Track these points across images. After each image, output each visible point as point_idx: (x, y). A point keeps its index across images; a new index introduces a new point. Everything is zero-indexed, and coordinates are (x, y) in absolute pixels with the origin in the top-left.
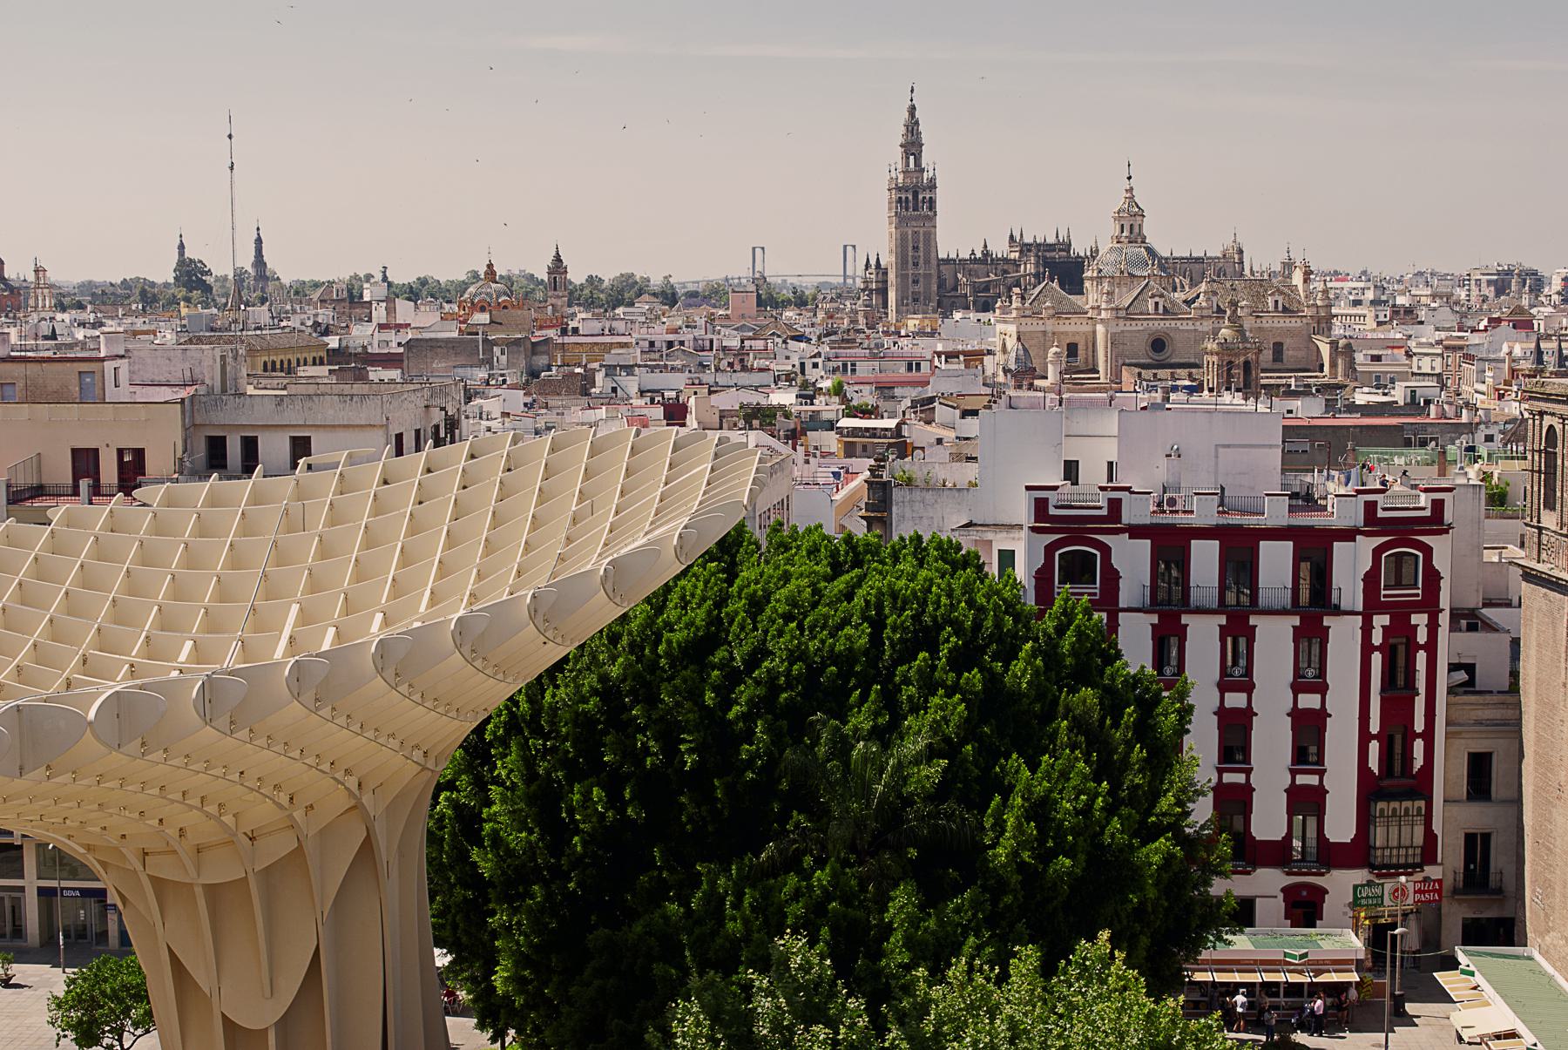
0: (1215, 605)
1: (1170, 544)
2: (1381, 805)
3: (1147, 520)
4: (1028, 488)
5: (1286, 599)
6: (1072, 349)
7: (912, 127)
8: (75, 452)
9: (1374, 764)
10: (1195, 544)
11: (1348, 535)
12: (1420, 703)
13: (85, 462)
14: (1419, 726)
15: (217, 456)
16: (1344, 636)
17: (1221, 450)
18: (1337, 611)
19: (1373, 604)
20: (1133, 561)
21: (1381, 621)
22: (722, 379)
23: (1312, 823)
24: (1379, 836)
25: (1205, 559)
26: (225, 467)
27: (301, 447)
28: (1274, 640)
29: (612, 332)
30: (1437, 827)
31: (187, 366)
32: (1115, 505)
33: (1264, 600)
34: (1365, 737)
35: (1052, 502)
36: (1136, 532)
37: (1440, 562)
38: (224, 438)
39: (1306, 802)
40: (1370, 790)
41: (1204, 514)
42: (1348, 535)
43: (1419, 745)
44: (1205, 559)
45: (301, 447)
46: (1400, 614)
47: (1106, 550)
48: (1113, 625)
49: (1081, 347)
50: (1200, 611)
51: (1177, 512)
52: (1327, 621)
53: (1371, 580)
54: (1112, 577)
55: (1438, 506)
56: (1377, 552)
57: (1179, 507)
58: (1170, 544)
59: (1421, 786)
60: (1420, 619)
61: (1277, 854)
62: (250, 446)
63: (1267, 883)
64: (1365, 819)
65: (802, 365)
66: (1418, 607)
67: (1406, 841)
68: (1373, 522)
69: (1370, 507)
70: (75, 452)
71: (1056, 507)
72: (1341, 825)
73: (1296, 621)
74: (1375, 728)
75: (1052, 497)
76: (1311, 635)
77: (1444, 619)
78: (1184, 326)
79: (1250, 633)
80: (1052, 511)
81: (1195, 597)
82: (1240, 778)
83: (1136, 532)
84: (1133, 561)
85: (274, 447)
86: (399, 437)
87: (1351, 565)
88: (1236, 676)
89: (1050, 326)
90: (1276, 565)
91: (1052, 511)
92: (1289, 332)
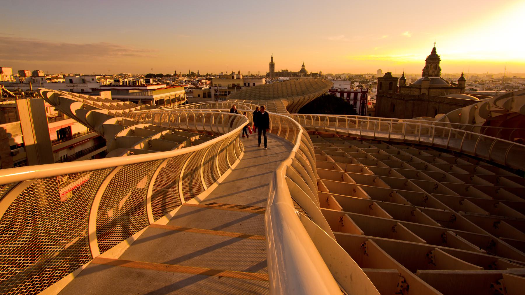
7: (272, 57)
11: (359, 92)
19: (361, 99)
20: (338, 95)
27: (254, 84)
36: (339, 92)
41: (346, 90)
42: (359, 92)
46: (364, 100)
53: (361, 97)
62: (249, 84)
68: (362, 92)
83: (339, 92)
85: (251, 84)
87: (359, 95)
90: (352, 95)
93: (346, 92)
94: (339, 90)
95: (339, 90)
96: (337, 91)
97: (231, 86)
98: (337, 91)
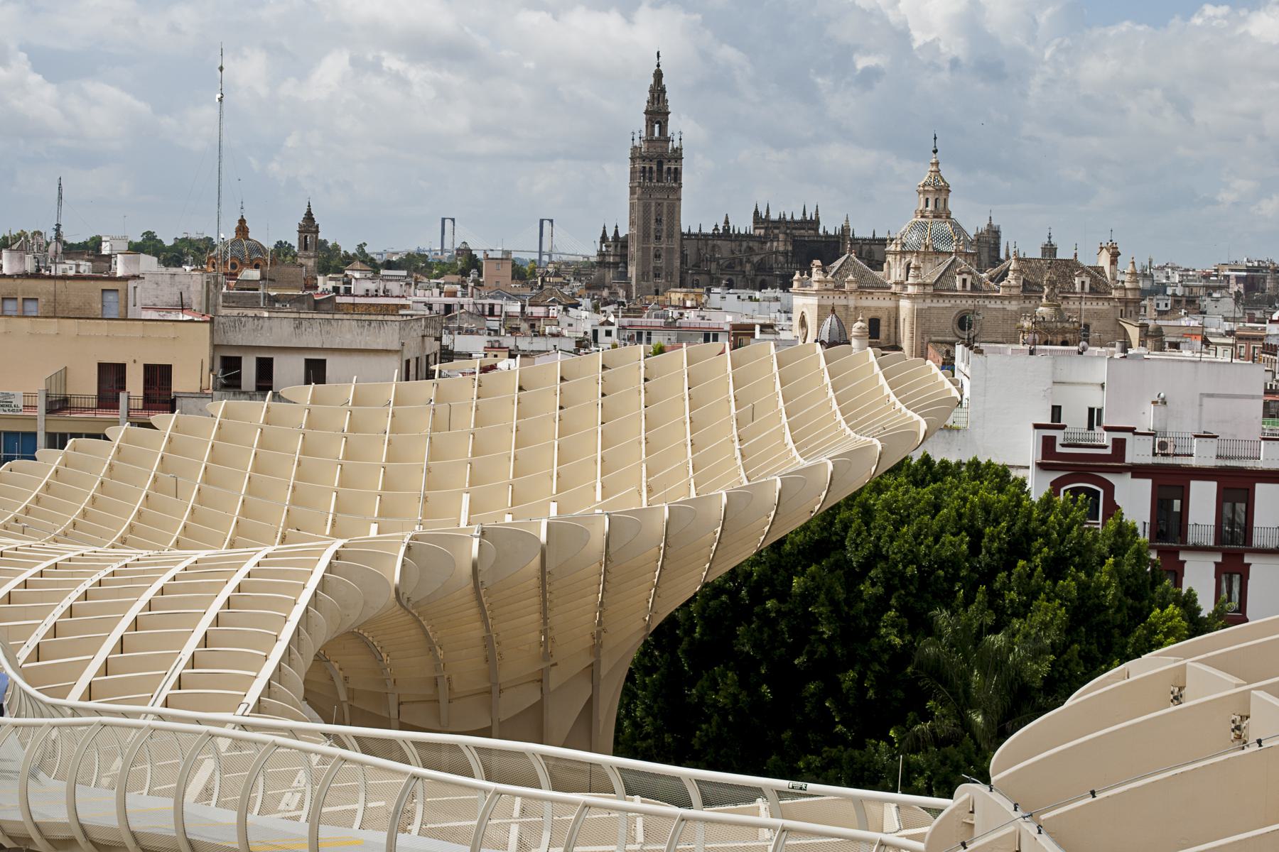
0: (1212, 543)
1: (1170, 483)
3: (1150, 460)
4: (1037, 426)
6: (874, 325)
8: (102, 367)
10: (1195, 485)
13: (112, 376)
15: (228, 374)
17: (1206, 400)
20: (1135, 500)
22: (524, 344)
25: (1203, 502)
26: (240, 387)
27: (315, 372)
29: (386, 294)
31: (176, 291)
32: (1119, 445)
33: (1257, 541)
35: (1060, 440)
36: (1138, 471)
38: (240, 358)
41: (1203, 456)
44: (1203, 502)
45: (315, 372)
47: (1109, 489)
49: (883, 323)
50: (1199, 549)
51: (1167, 455)
57: (1170, 450)
58: (1170, 483)
62: (265, 368)
65: (595, 332)
70: (102, 367)
71: (1063, 445)
75: (1060, 436)
78: (992, 304)
80: (1059, 449)
83: (1138, 471)
85: (288, 369)
86: (408, 362)
89: (852, 301)
91: (1059, 449)
92: (1097, 314)
93: (1203, 474)
94: (1138, 452)
95: (1138, 452)
97: (86, 385)
98: (1116, 459)
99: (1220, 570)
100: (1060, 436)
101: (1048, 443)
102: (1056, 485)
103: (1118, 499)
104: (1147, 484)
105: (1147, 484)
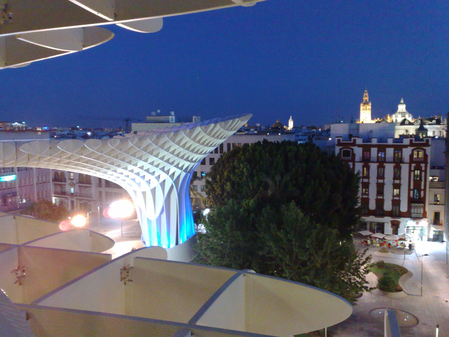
1: (366, 148)
2: (413, 204)
5: (392, 160)
9: (411, 195)
11: (406, 146)
12: (423, 183)
14: (422, 188)
16: (405, 168)
18: (403, 163)
20: (358, 152)
21: (413, 165)
23: (397, 207)
24: (413, 211)
28: (389, 169)
30: (427, 210)
32: (355, 141)
34: (409, 190)
37: (428, 153)
39: (396, 203)
40: (411, 201)
43: (422, 193)
47: (352, 150)
48: (354, 165)
50: (373, 162)
52: (401, 165)
53: (411, 156)
54: (354, 155)
55: (427, 141)
56: (413, 151)
59: (422, 201)
60: (423, 165)
61: (390, 214)
63: (387, 220)
64: (409, 207)
66: (422, 162)
67: (419, 212)
68: (411, 144)
69: (411, 141)
72: (404, 208)
73: (394, 164)
74: (412, 187)
75: (341, 139)
76: (398, 168)
77: (429, 165)
79: (384, 167)
81: (372, 159)
82: (381, 197)
83: (359, 146)
84: (358, 152)
88: (381, 176)
91: (341, 142)
93: (374, 146)
95: (359, 141)
96: (354, 144)
98: (354, 144)
99: (378, 167)
100: (341, 139)
101: (339, 140)
102: (340, 150)
103: (355, 152)
104: (361, 149)
105: (361, 149)
